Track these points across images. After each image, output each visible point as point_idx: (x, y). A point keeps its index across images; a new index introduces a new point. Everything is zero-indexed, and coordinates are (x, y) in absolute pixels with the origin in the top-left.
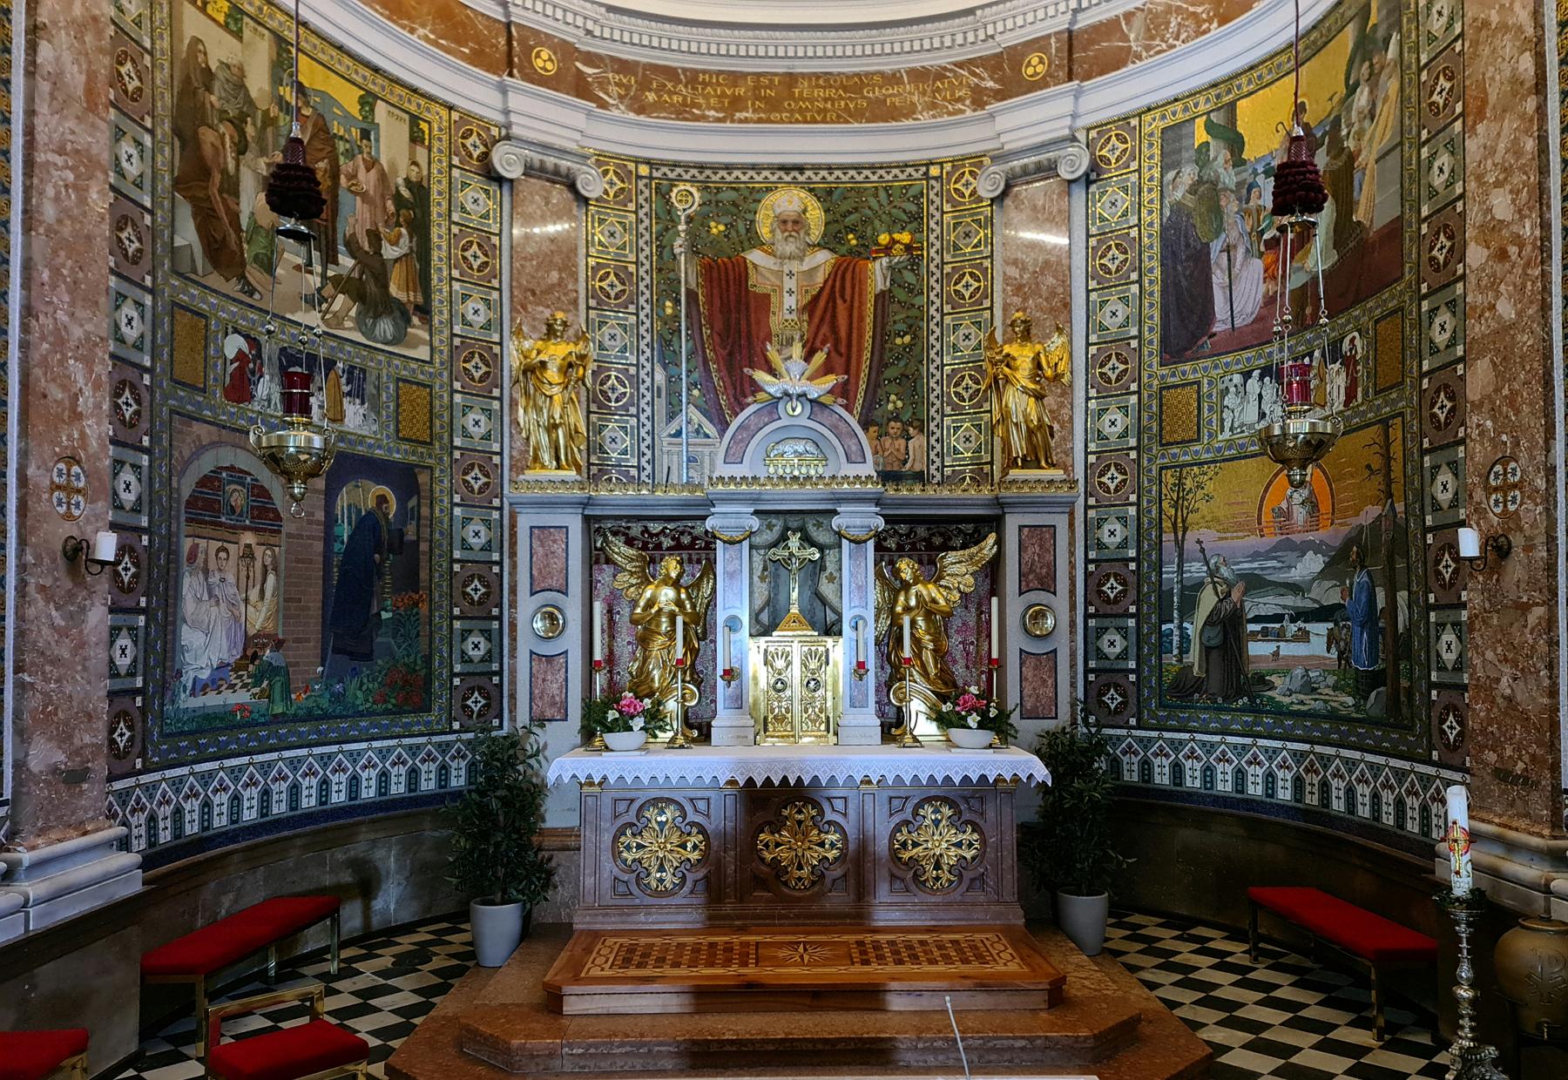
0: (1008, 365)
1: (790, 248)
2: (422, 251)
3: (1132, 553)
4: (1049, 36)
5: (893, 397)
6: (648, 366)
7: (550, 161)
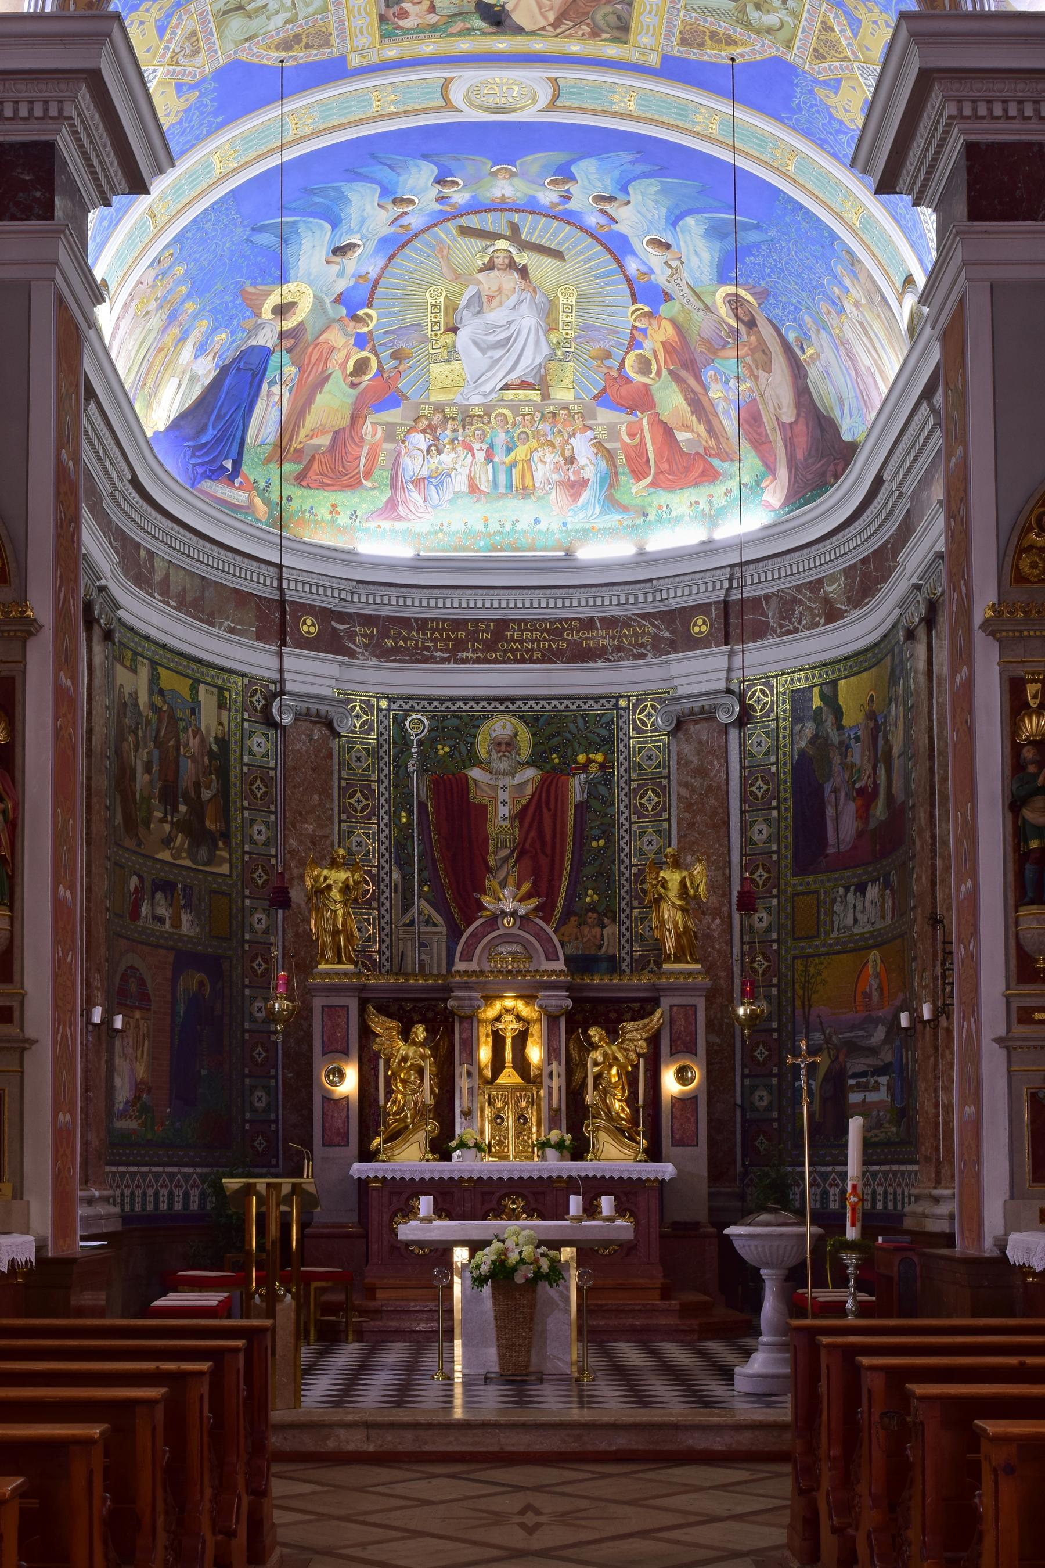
0: (663, 886)
1: (503, 766)
2: (224, 792)
3: (775, 1025)
4: (710, 604)
5: (590, 892)
6: (387, 867)
7: (314, 707)
